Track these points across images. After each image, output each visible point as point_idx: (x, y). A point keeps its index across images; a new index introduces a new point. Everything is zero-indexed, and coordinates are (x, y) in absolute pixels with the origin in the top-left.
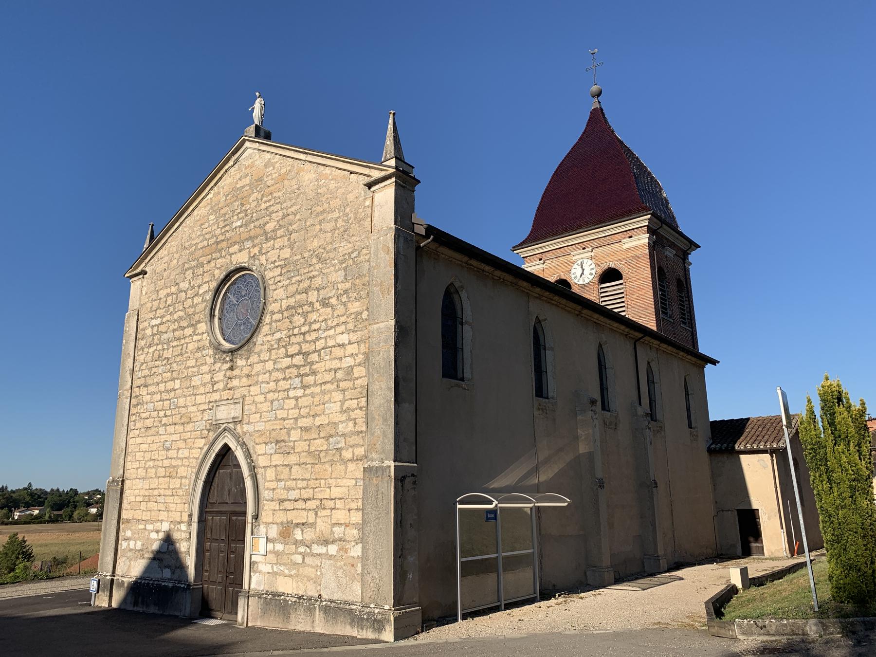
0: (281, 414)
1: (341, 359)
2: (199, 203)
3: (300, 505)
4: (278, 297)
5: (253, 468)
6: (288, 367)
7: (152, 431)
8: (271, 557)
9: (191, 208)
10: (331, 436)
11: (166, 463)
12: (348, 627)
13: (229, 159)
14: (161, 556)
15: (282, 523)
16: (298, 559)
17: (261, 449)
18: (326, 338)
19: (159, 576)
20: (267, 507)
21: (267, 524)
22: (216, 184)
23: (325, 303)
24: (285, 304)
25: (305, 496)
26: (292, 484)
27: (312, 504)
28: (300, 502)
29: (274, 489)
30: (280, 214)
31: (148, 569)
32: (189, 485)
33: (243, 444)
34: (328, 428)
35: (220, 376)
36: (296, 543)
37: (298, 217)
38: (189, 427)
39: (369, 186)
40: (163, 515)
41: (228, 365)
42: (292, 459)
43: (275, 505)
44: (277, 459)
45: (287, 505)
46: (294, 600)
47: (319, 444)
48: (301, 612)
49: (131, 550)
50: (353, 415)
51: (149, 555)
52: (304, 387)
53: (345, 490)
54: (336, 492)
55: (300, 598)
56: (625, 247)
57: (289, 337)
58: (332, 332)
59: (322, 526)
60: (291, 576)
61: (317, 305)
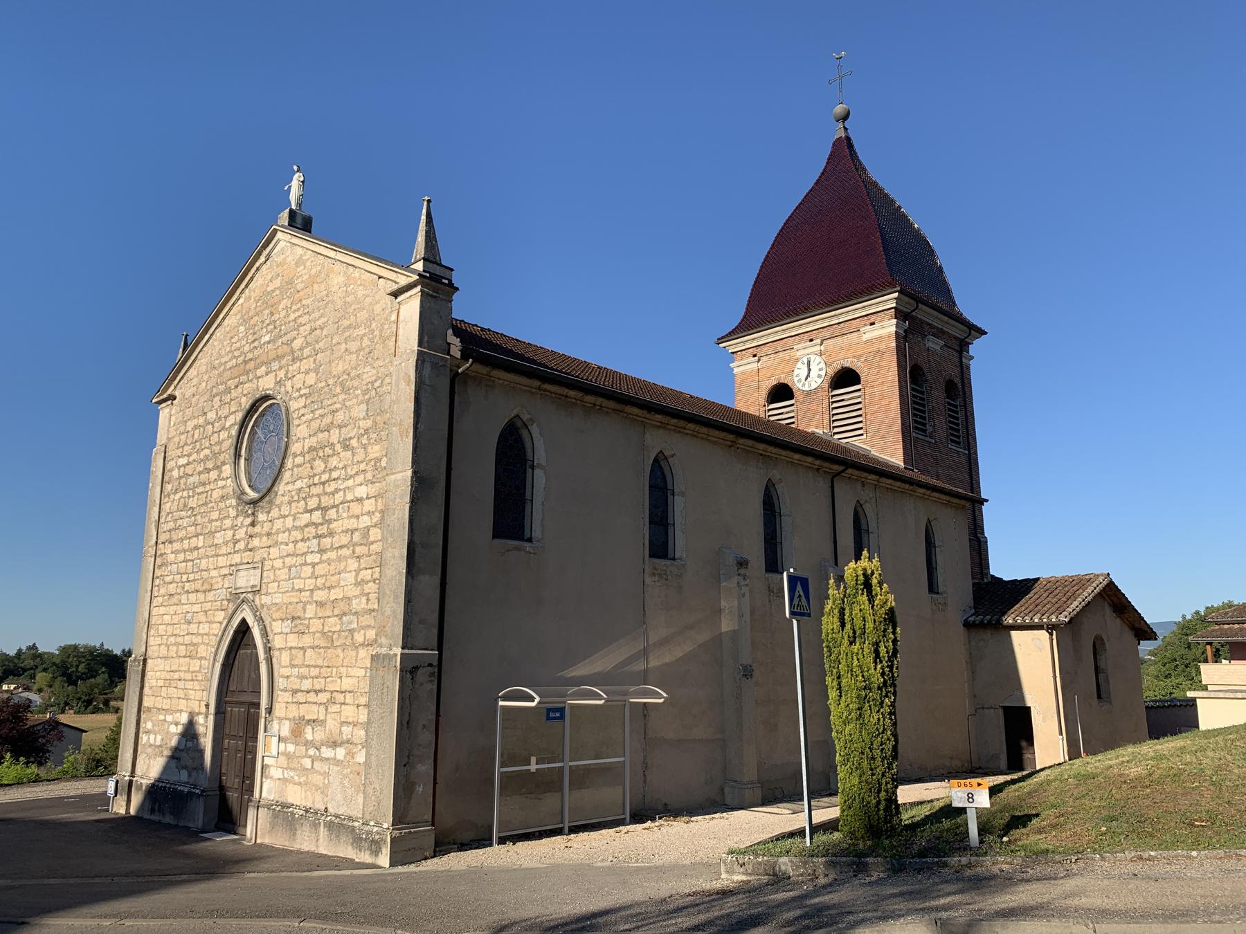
0: (298, 584)
1: (358, 517)
2: (230, 309)
3: (312, 697)
4: (302, 435)
5: (268, 650)
6: (307, 526)
7: (175, 600)
8: (282, 759)
9: (221, 316)
10: (345, 614)
11: (188, 639)
12: (350, 848)
13: (260, 253)
14: (177, 755)
16: (307, 763)
17: (277, 627)
18: (344, 490)
20: (282, 698)
21: (280, 719)
22: (247, 286)
23: (346, 447)
24: (307, 444)
25: (317, 687)
26: (304, 671)
27: (323, 697)
28: (312, 694)
30: (308, 327)
31: (166, 769)
33: (260, 620)
34: (342, 604)
35: (241, 534)
36: (307, 744)
37: (325, 332)
38: (210, 596)
39: (395, 294)
40: (183, 704)
41: (249, 520)
42: (307, 640)
43: (287, 697)
44: (293, 641)
45: (300, 697)
46: (301, 812)
47: (333, 624)
48: (306, 827)
49: (151, 745)
50: (367, 588)
51: (167, 753)
52: (322, 551)
54: (347, 683)
55: (307, 811)
56: (865, 337)
57: (309, 487)
58: (350, 483)
59: (331, 724)
60: (300, 784)
61: (338, 447)
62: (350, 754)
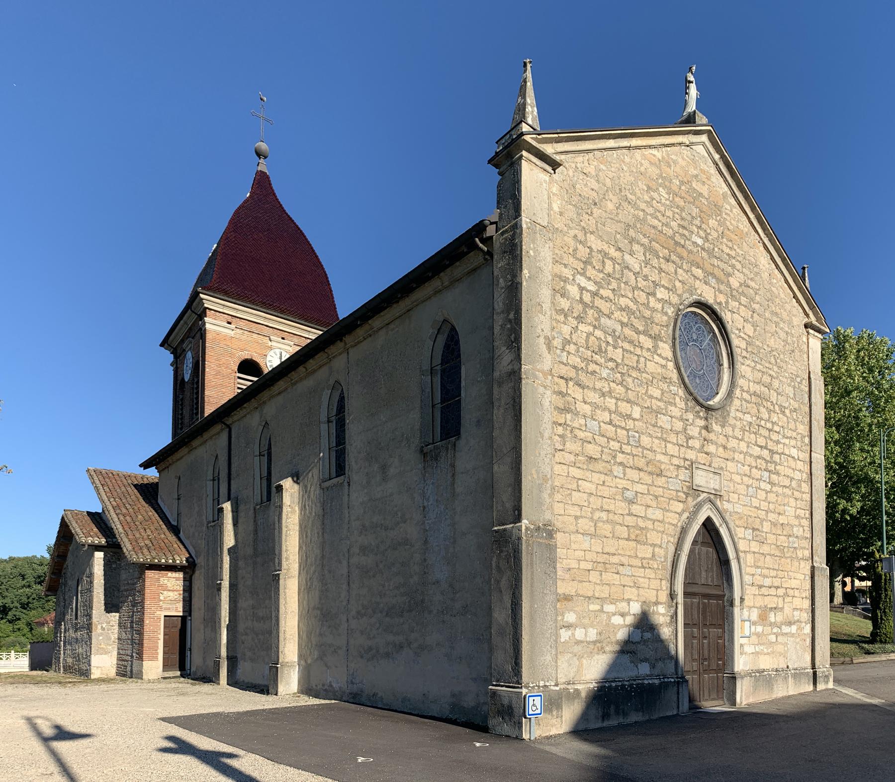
3: (773, 591)
8: (754, 639)
10: (790, 536)
14: (632, 647)
15: (760, 608)
17: (740, 532)
19: (633, 674)
20: (750, 591)
25: (776, 584)
27: (781, 592)
28: (773, 589)
29: (753, 575)
31: (613, 667)
32: (666, 558)
36: (771, 624)
40: (630, 593)
42: (766, 549)
43: (755, 590)
44: (755, 547)
48: (780, 681)
49: (578, 642)
51: (612, 648)
53: (798, 582)
54: (794, 583)
59: (787, 610)
60: (768, 654)
62: (800, 629)
